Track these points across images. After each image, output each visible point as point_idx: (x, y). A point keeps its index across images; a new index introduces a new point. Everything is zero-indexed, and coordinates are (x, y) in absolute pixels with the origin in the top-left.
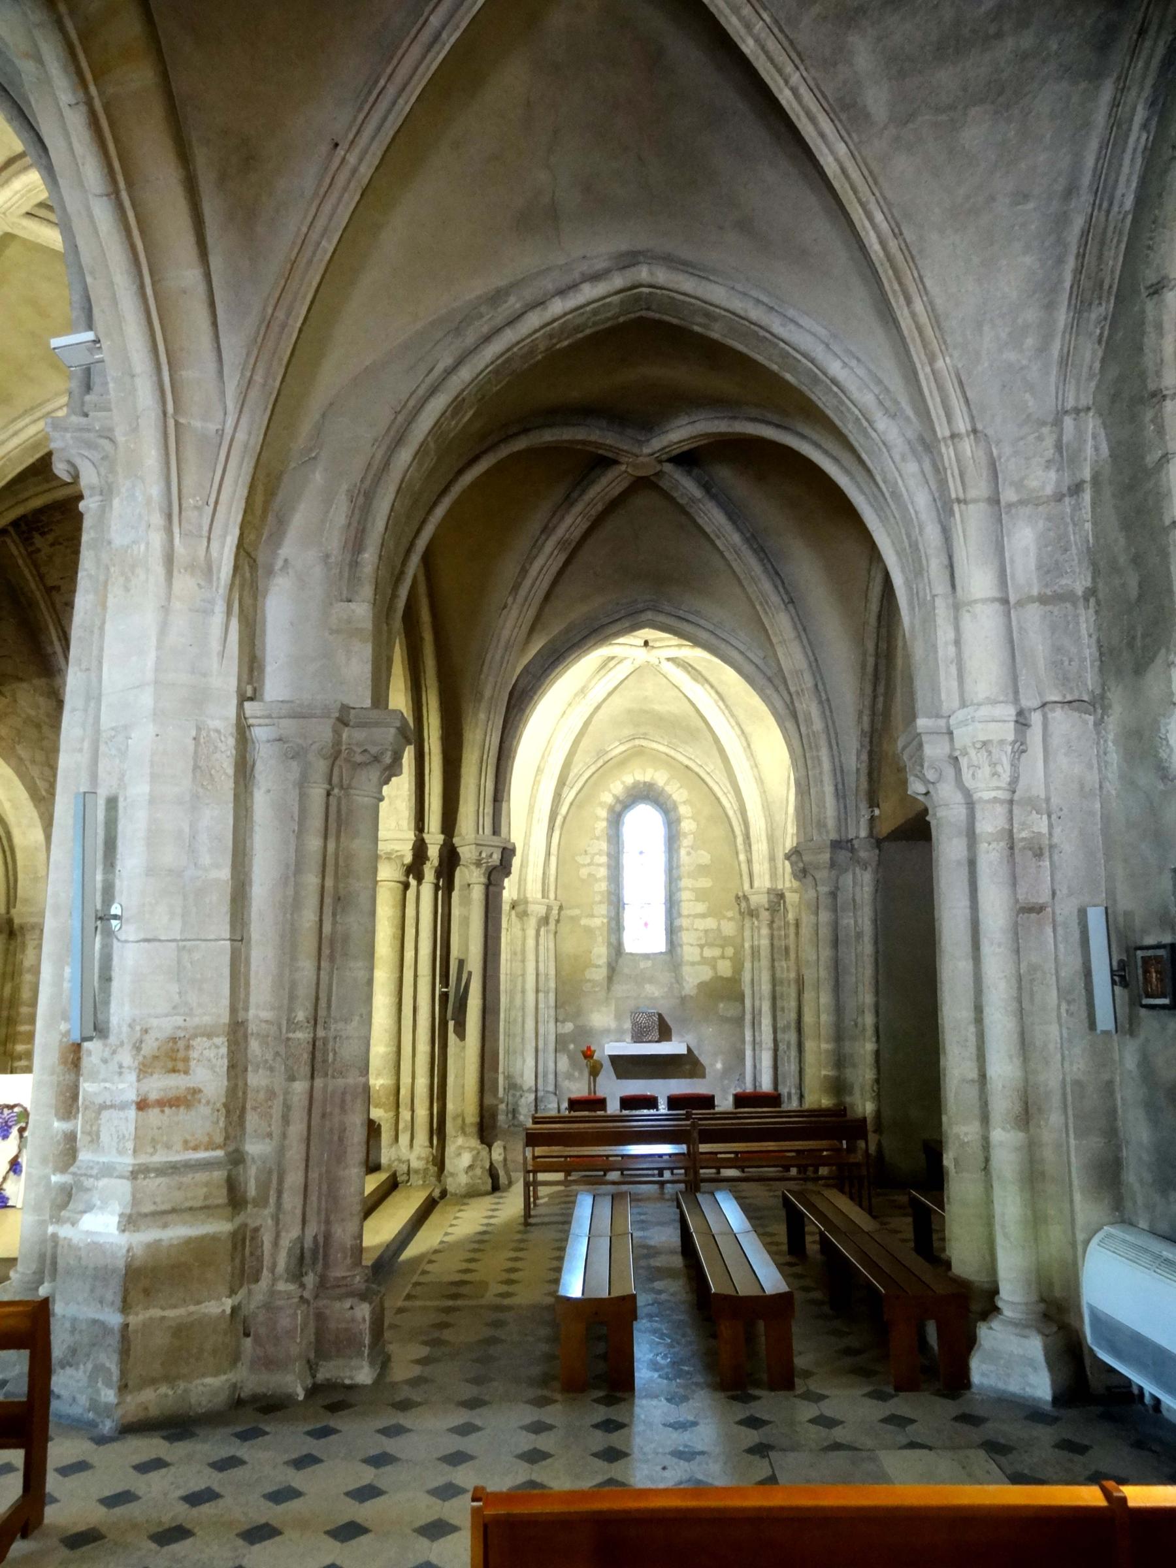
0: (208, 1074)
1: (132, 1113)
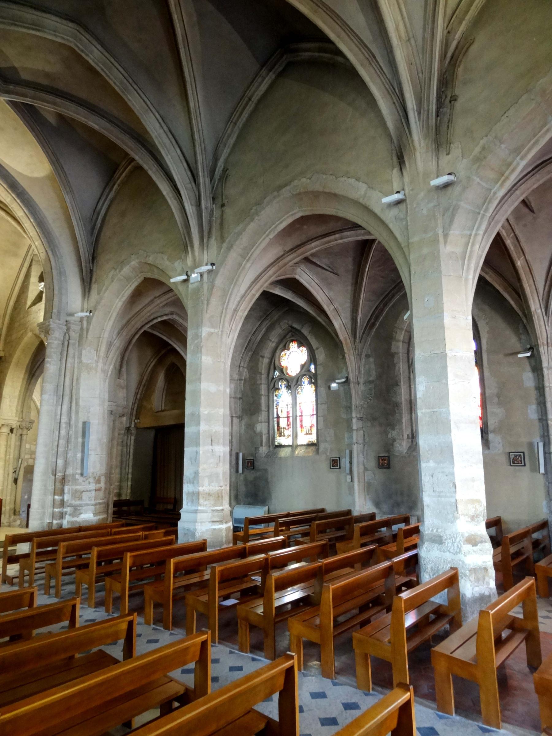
0: (102, 485)
1: (94, 492)
